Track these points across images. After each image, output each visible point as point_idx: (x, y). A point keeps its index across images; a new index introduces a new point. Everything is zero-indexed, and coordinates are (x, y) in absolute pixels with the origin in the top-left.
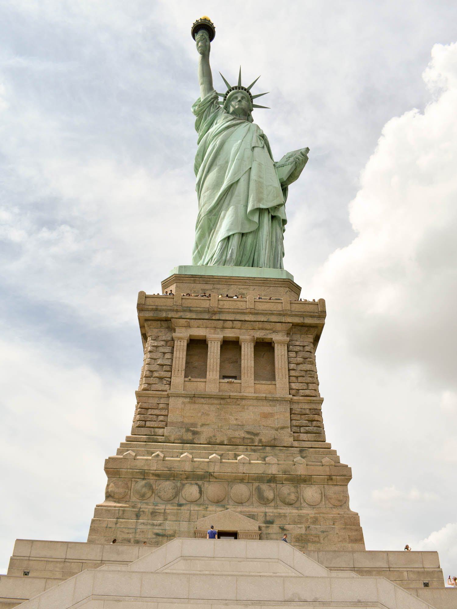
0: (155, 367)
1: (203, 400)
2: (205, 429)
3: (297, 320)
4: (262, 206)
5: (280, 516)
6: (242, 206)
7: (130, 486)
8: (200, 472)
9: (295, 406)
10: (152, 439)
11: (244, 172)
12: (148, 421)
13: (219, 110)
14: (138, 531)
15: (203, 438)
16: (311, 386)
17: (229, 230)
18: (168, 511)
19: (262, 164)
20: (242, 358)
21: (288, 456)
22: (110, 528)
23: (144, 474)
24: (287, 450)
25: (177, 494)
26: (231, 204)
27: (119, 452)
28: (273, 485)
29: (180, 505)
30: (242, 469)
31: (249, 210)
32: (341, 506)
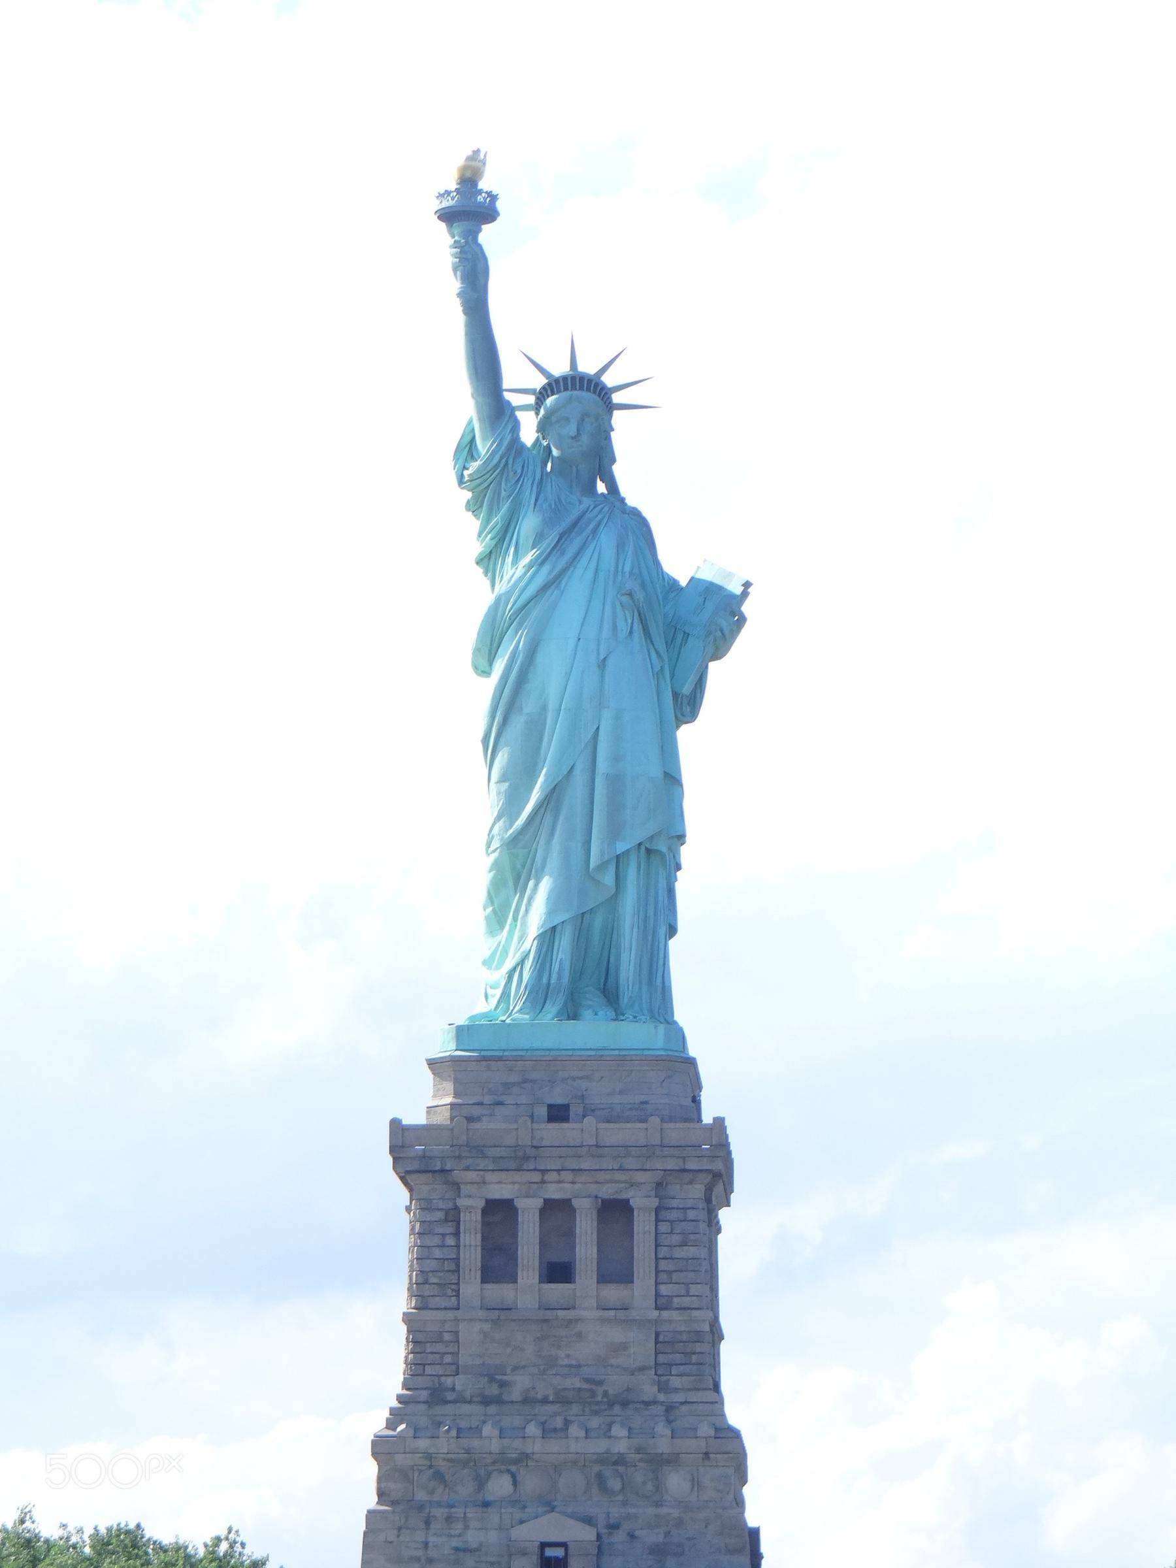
3: (672, 1164)
4: (621, 847)
5: (629, 1517)
6: (580, 844)
7: (411, 1477)
12: (426, 1364)
13: (523, 481)
14: (430, 1544)
15: (516, 1394)
16: (694, 1289)
20: (577, 1241)
22: (391, 1542)
24: (647, 1409)
27: (391, 1425)
28: (621, 1469)
29: (486, 1505)
31: (592, 866)
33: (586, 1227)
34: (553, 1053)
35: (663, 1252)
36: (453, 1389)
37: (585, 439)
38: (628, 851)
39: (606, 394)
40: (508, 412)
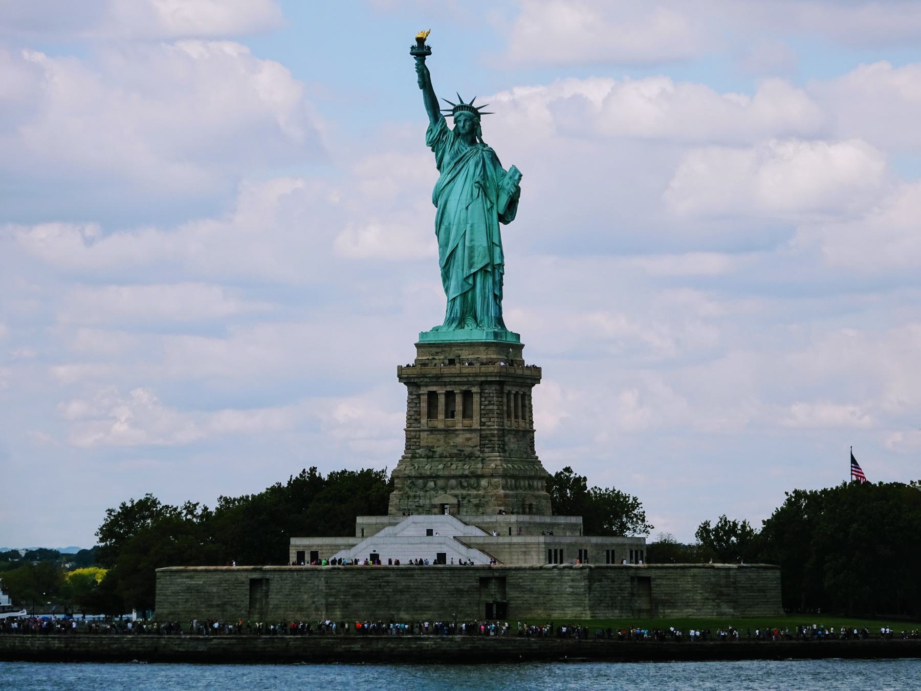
0: (412, 413)
1: (437, 433)
3: (483, 379)
4: (473, 271)
5: (469, 495)
10: (413, 457)
15: (437, 456)
16: (492, 420)
17: (454, 293)
18: (421, 495)
21: (476, 463)
23: (409, 477)
25: (425, 485)
26: (454, 268)
27: (399, 465)
28: (467, 479)
29: (427, 491)
30: (453, 473)
33: (459, 399)
34: (451, 342)
36: (418, 454)
37: (467, 127)
38: (477, 272)
40: (440, 120)
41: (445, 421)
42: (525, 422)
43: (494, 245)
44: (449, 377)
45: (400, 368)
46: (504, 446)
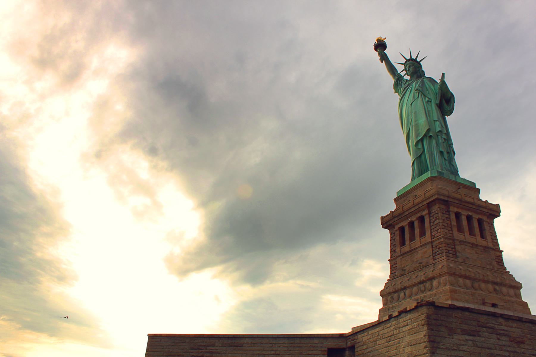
1: (405, 255)
2: (407, 267)
3: (428, 201)
4: (419, 138)
8: (403, 287)
9: (434, 244)
11: (410, 123)
15: (407, 272)
16: (439, 231)
19: (417, 111)
23: (390, 293)
25: (399, 297)
28: (424, 284)
29: (400, 302)
32: (446, 285)
33: (416, 225)
35: (432, 224)
39: (414, 60)
41: (410, 245)
42: (487, 241)
43: (435, 122)
44: (408, 210)
45: (382, 218)
46: (456, 253)
